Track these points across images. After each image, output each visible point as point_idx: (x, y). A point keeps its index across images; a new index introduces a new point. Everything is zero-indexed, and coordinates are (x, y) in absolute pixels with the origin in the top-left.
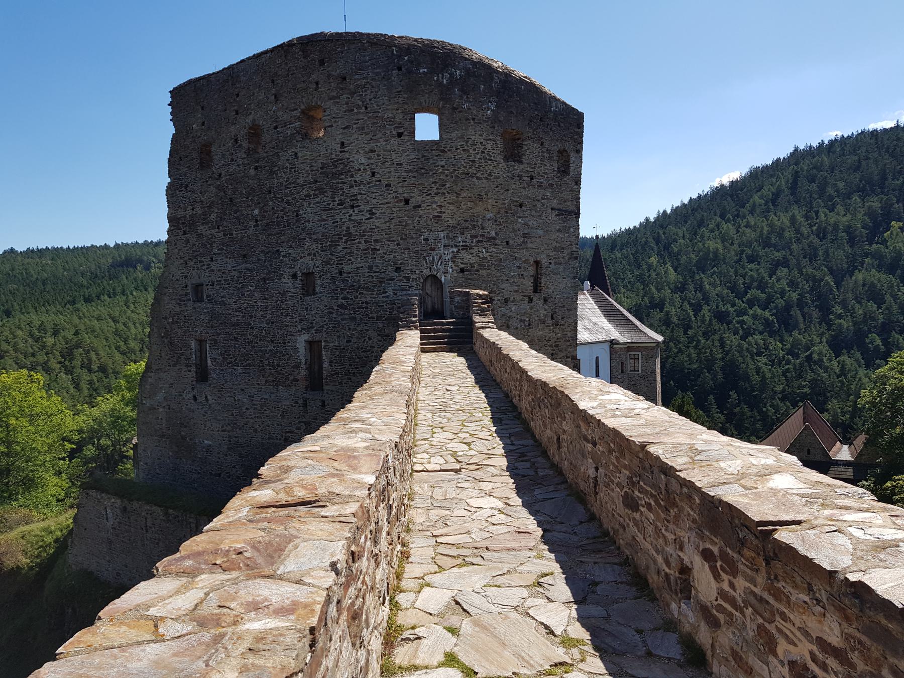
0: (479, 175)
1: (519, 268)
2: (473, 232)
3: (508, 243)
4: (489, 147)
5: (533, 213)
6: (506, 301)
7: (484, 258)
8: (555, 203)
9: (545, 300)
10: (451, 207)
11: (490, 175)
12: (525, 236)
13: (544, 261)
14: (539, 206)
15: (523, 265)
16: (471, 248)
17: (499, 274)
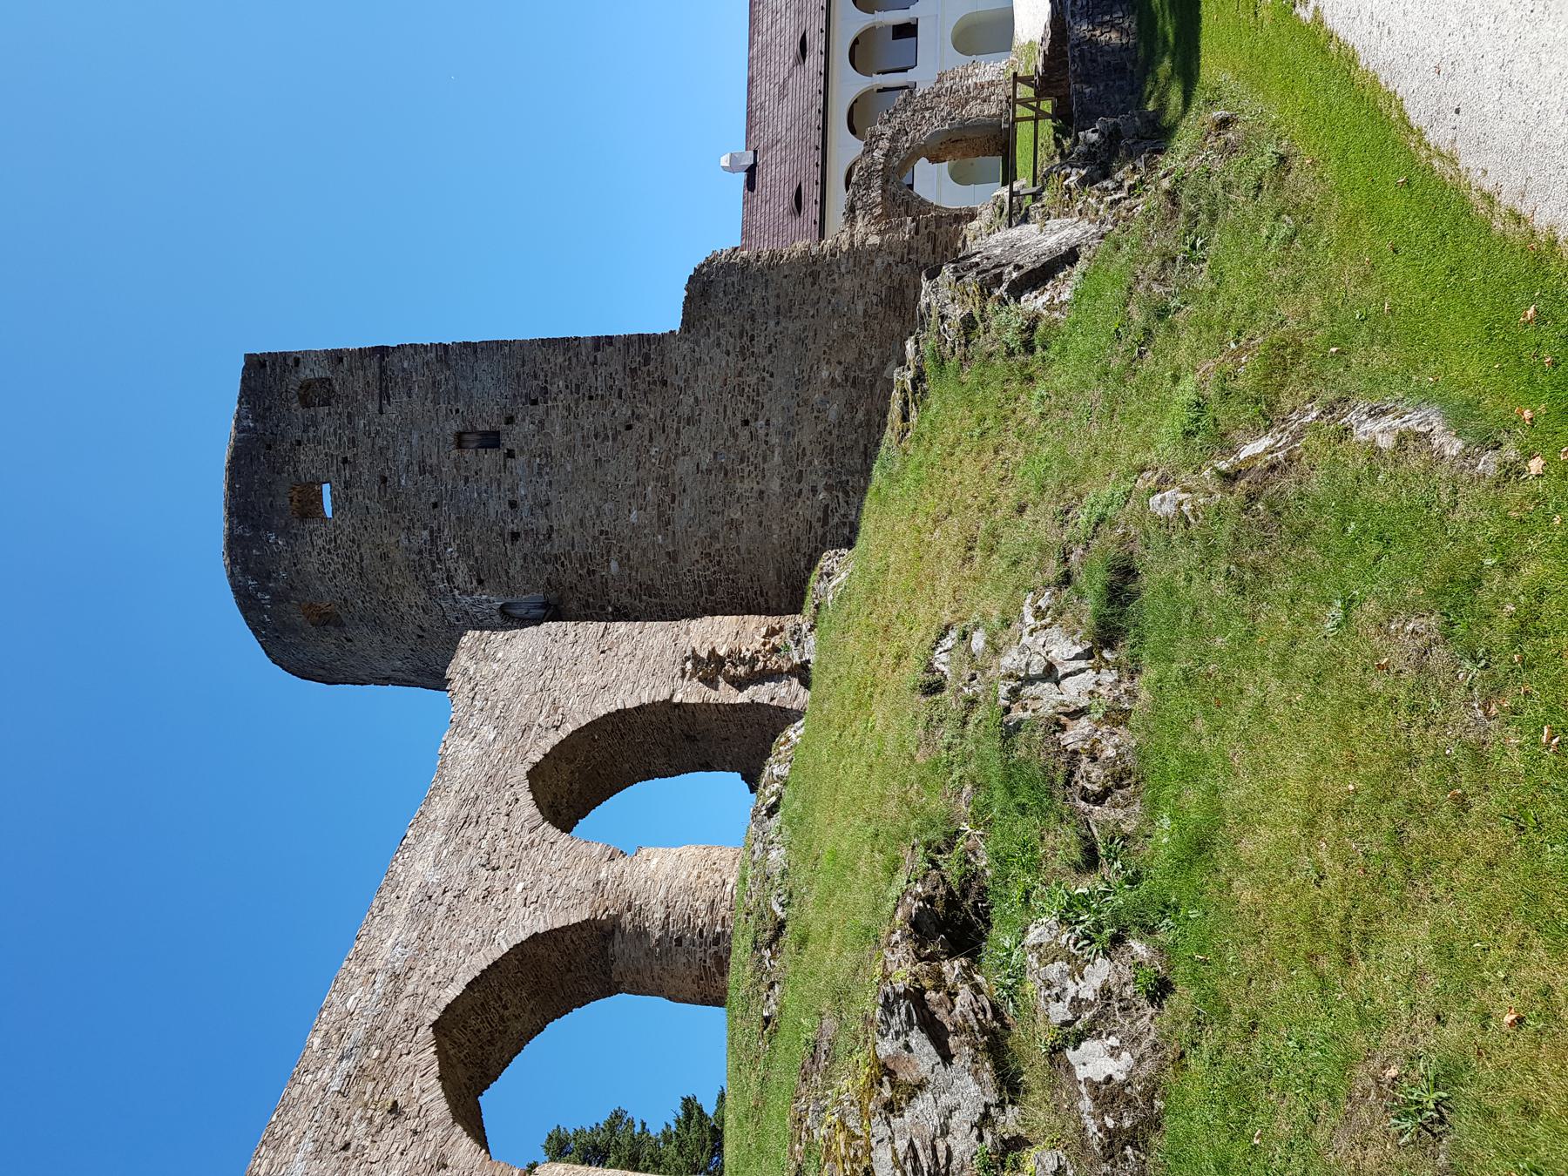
0: (357, 558)
1: (467, 480)
2: (429, 568)
3: (435, 505)
4: (320, 542)
5: (390, 454)
6: (513, 505)
7: (458, 550)
8: (372, 407)
9: (510, 420)
10: (406, 595)
11: (353, 541)
12: (422, 472)
13: (454, 426)
14: (380, 442)
15: (462, 472)
16: (448, 570)
17: (477, 521)
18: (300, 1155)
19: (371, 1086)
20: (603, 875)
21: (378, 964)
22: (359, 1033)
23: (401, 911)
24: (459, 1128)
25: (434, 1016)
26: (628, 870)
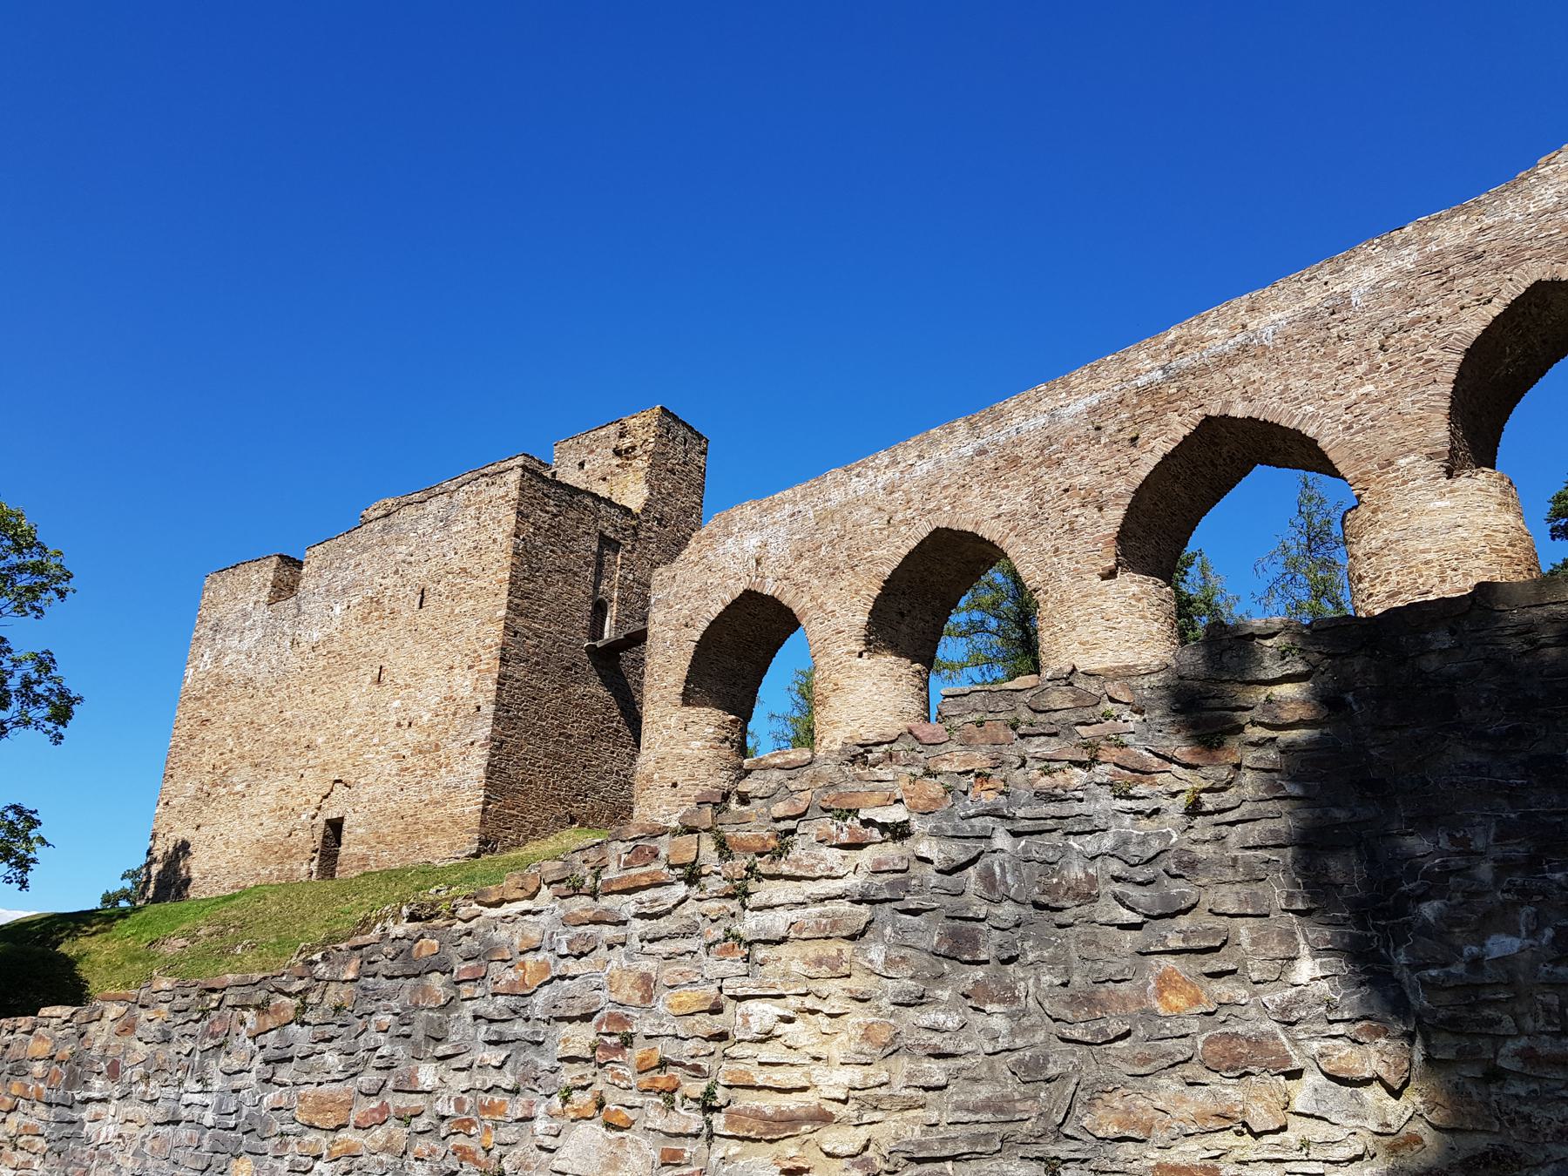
18: (1088, 400)
19: (1149, 407)
20: (1402, 462)
21: (1251, 326)
22: (1186, 362)
23: (1314, 296)
24: (1128, 500)
25: (1214, 412)
26: (1419, 482)
